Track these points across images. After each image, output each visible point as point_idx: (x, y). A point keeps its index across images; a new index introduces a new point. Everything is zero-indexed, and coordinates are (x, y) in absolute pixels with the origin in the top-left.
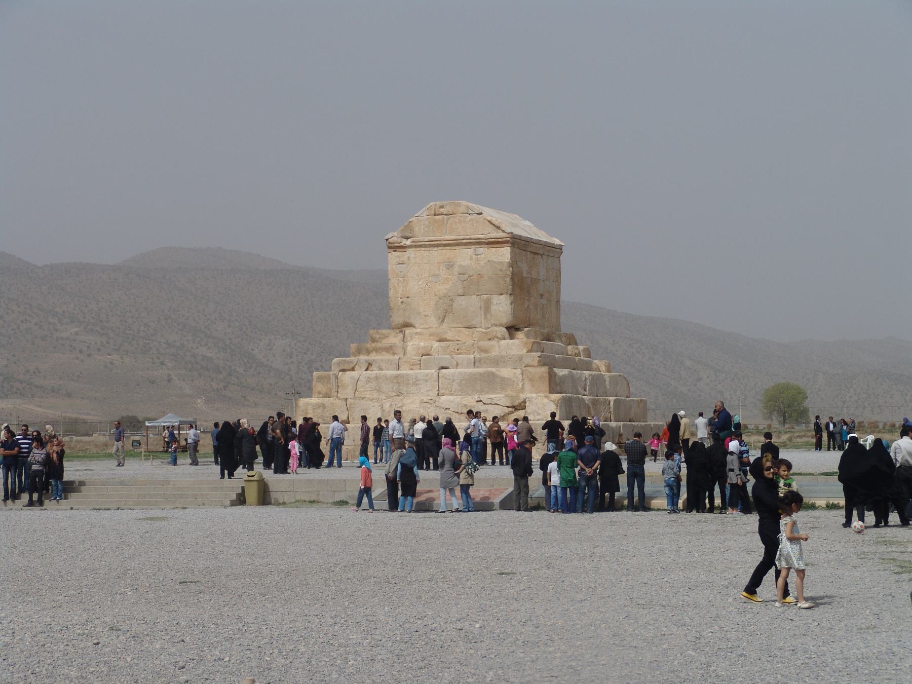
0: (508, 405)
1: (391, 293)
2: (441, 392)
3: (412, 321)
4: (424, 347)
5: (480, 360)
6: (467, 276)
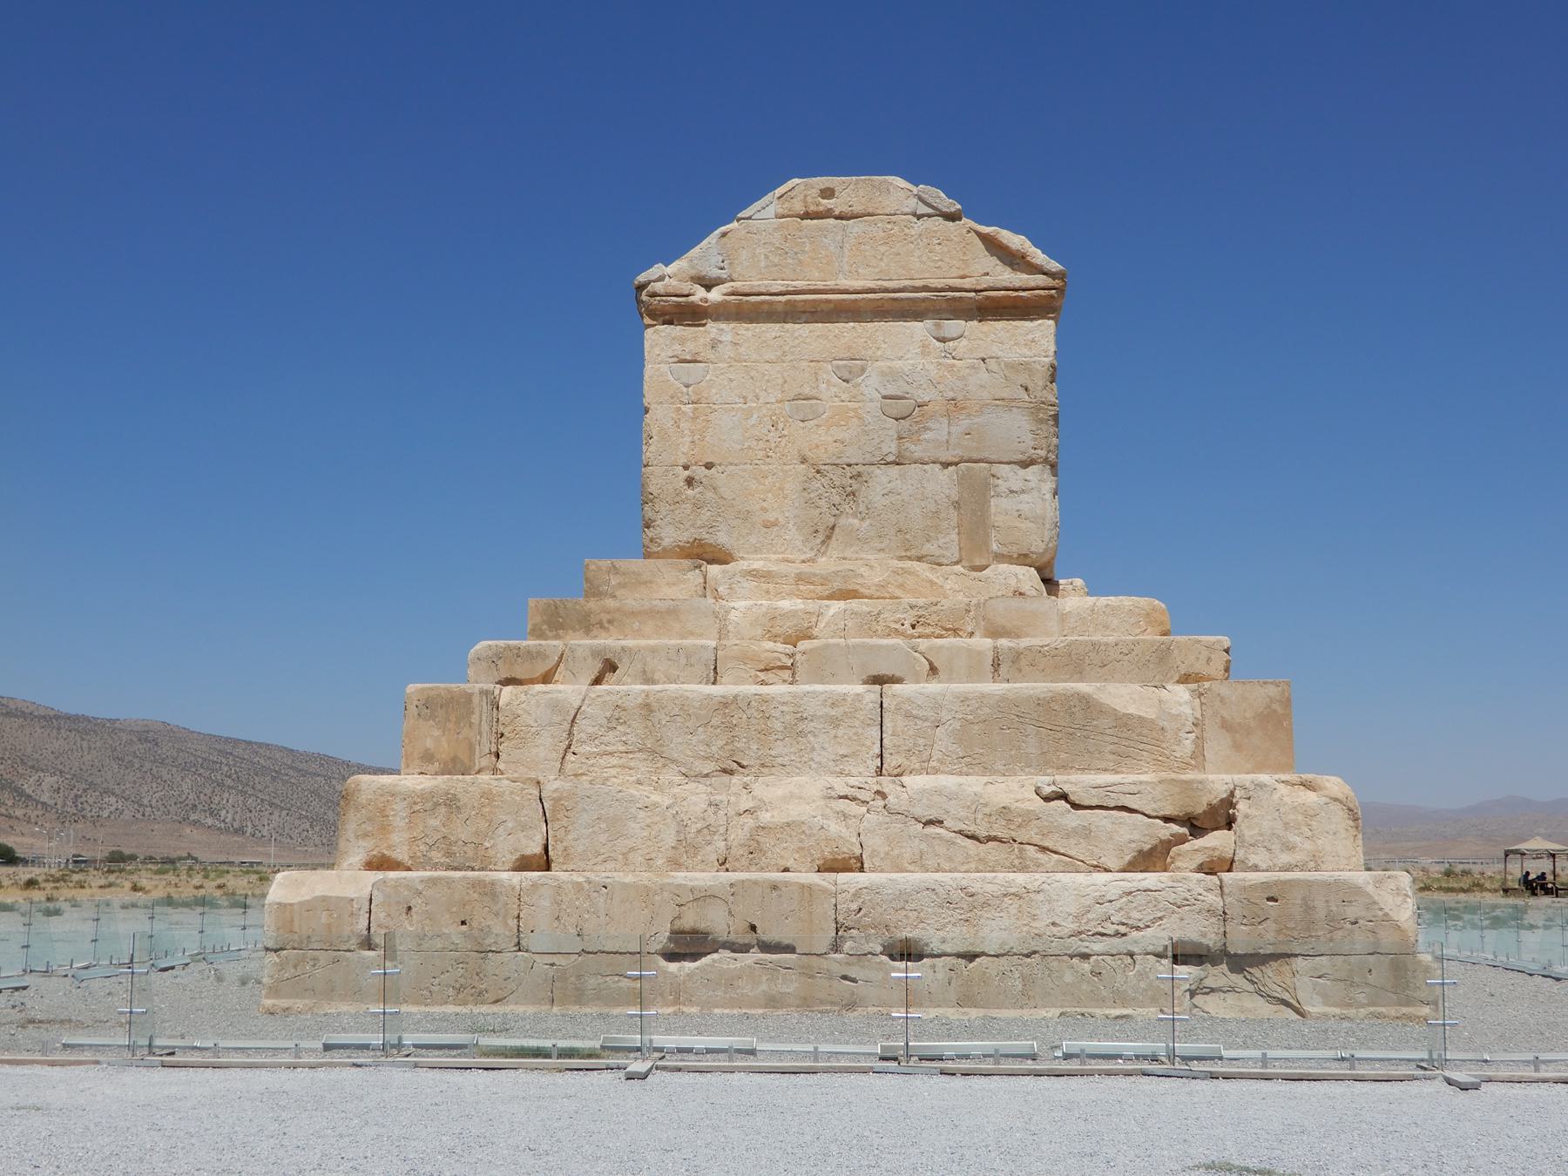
0: (1168, 811)
1: (650, 451)
2: (891, 762)
3: (722, 538)
4: (793, 614)
5: (1017, 656)
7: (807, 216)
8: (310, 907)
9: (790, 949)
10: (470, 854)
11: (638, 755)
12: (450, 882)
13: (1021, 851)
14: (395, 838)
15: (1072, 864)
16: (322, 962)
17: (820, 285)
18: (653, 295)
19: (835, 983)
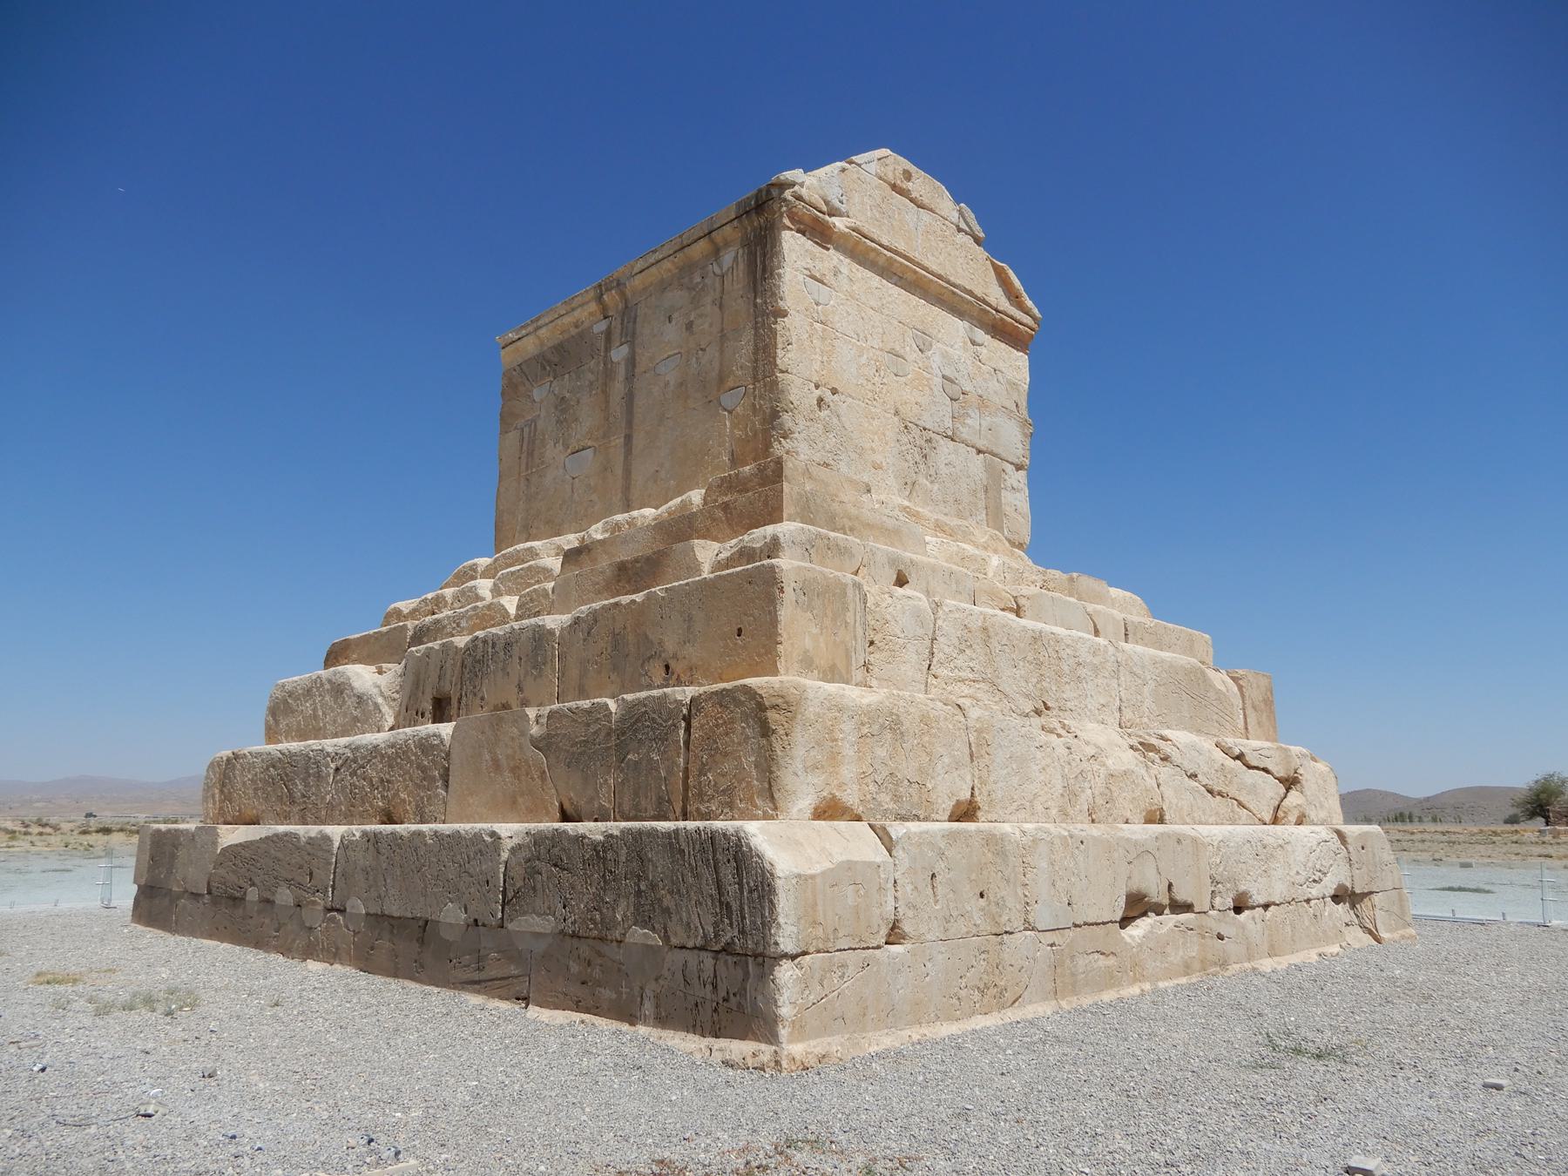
0: (1282, 774)
10: (915, 799)
11: (982, 685)
14: (848, 772)
16: (850, 971)
17: (916, 255)
18: (799, 198)
19: (1209, 941)
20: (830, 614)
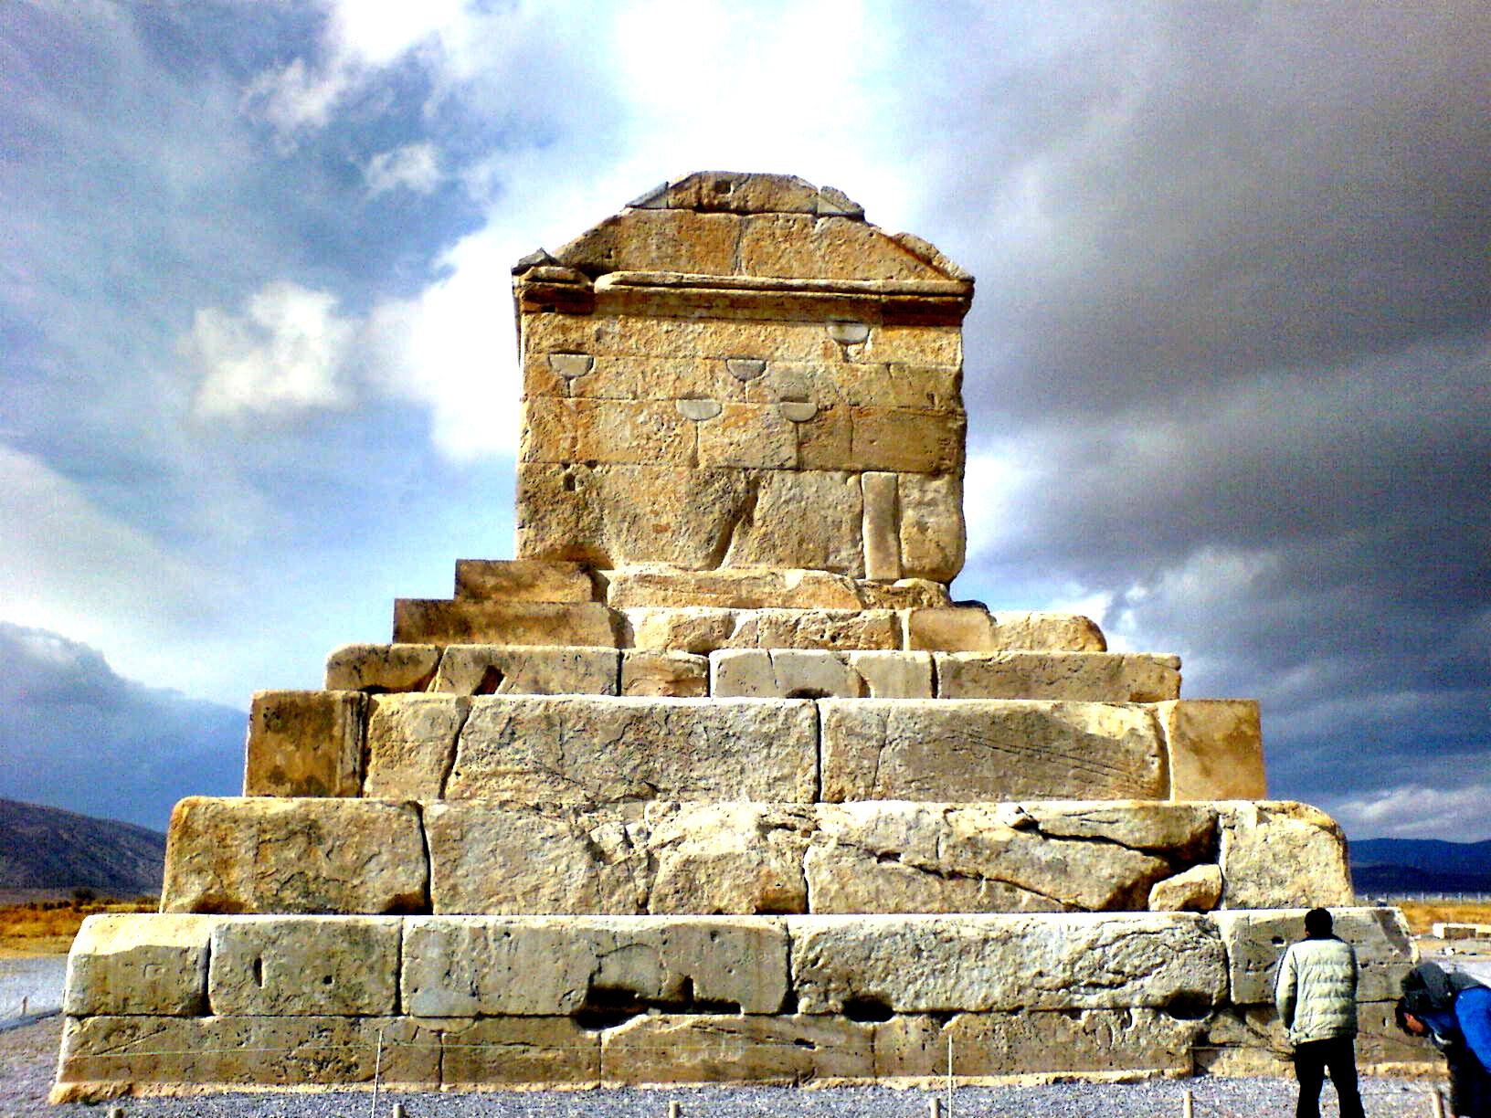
5: (957, 670)
6: (811, 407)
7: (700, 208)
8: (128, 960)
9: (734, 1008)
12: (310, 928)
13: (991, 889)
14: (236, 874)
15: (1049, 904)
16: (143, 1032)
20: (309, 730)
